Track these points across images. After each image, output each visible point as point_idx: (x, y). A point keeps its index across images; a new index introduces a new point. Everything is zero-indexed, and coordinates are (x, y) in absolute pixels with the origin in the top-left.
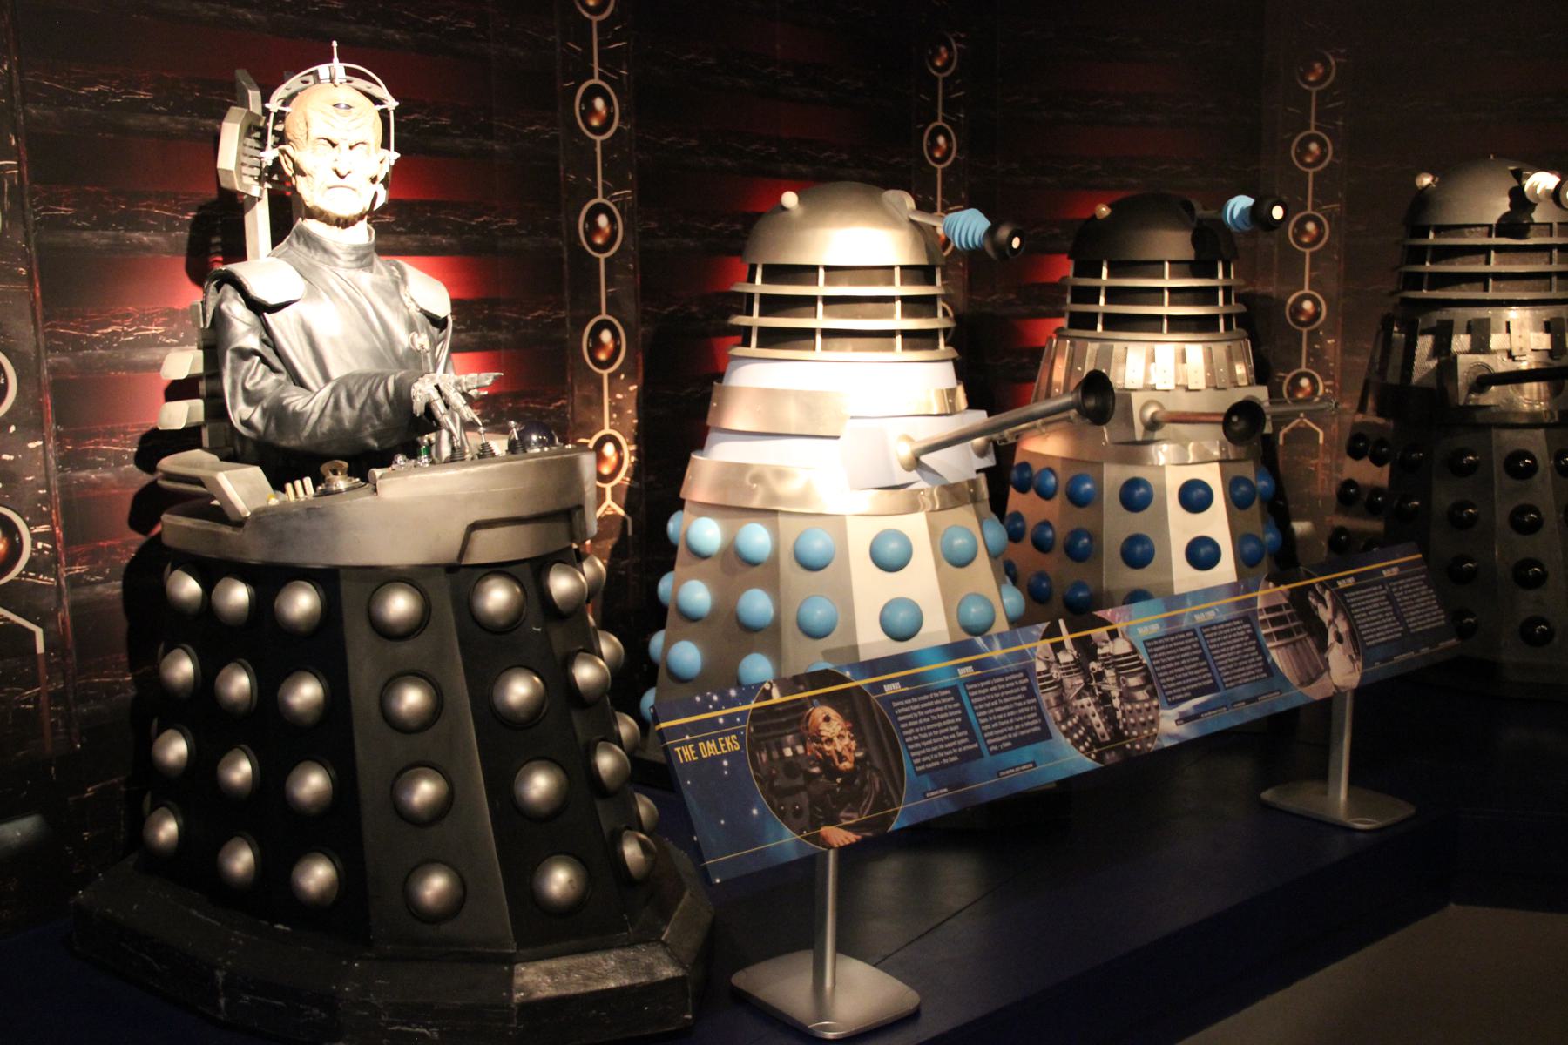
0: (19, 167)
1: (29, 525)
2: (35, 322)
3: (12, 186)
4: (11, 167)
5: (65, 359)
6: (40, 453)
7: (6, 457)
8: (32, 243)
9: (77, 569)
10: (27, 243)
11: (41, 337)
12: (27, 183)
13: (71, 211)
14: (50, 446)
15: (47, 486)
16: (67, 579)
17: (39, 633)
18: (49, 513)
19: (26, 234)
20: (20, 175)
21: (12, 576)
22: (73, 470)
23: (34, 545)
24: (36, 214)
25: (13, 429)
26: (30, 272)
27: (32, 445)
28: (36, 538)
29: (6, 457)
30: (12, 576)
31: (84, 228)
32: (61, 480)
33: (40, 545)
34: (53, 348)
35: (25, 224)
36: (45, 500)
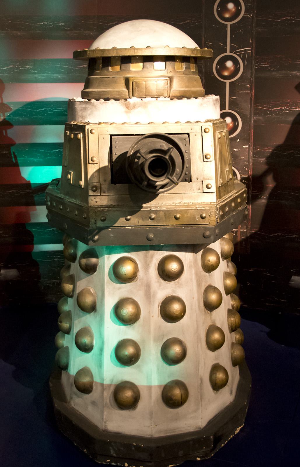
0: (252, 50)
1: (240, 173)
2: (251, 104)
3: (248, 56)
4: (249, 50)
5: (260, 118)
6: (247, 150)
7: (235, 149)
10: (251, 77)
11: (253, 109)
12: (254, 55)
13: (269, 65)
14: (251, 148)
15: (248, 161)
16: (252, 195)
18: (248, 171)
19: (251, 73)
20: (252, 52)
22: (259, 157)
24: (256, 66)
25: (238, 140)
26: (251, 86)
27: (244, 147)
29: (235, 149)
31: (274, 71)
32: (253, 160)
34: (255, 114)
35: (251, 70)
36: (247, 166)
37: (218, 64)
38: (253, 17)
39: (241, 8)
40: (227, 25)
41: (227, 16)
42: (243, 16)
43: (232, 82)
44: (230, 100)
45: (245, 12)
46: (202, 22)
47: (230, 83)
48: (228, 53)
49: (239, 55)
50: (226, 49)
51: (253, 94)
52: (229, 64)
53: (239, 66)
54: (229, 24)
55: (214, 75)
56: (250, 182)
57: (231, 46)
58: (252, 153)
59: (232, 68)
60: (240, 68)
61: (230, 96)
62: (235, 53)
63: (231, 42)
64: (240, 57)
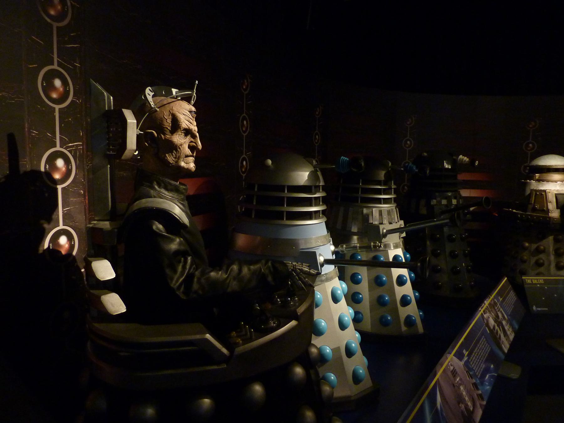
0: (82, 145)
2: (85, 215)
8: (86, 180)
20: (83, 149)
24: (88, 166)
26: (84, 192)
37: (47, 162)
38: (81, 103)
39: (69, 88)
40: (54, 108)
41: (54, 96)
42: (72, 101)
43: (64, 188)
46: (23, 98)
47: (62, 188)
48: (58, 148)
50: (55, 143)
53: (71, 166)
59: (64, 169)
60: (71, 168)
61: (63, 207)
62: (66, 149)
63: (60, 133)
64: (71, 154)
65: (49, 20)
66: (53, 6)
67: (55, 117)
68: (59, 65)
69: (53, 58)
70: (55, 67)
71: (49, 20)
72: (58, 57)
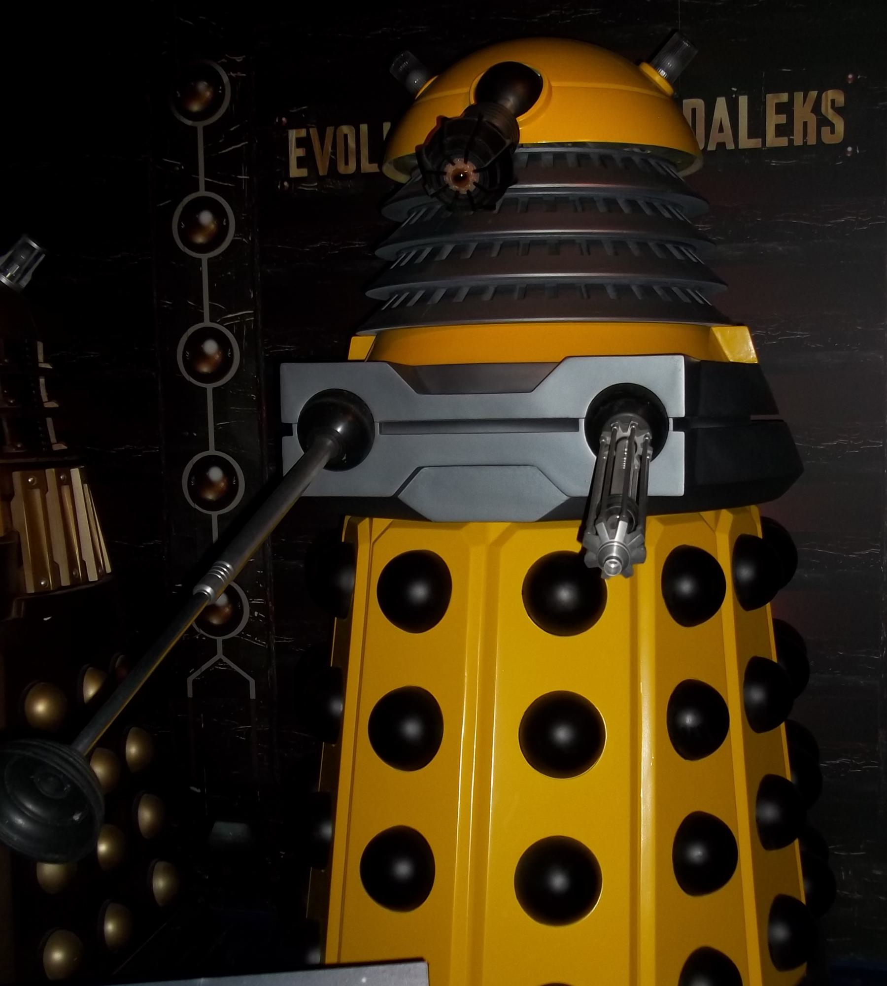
0: (254, 315)
9: (285, 640)
17: (252, 682)
20: (255, 321)
21: (234, 634)
23: (252, 613)
28: (253, 608)
30: (234, 634)
33: (256, 614)
40: (200, 260)
41: (200, 239)
42: (233, 242)
44: (216, 428)
45: (237, 231)
47: (214, 389)
49: (229, 328)
51: (264, 415)
52: (211, 347)
54: (204, 257)
55: (181, 373)
56: (271, 617)
57: (212, 308)
58: (270, 550)
60: (232, 355)
61: (216, 420)
62: (221, 323)
65: (189, 123)
66: (195, 94)
67: (201, 273)
68: (209, 187)
69: (198, 180)
70: (202, 192)
71: (189, 123)
72: (206, 176)
